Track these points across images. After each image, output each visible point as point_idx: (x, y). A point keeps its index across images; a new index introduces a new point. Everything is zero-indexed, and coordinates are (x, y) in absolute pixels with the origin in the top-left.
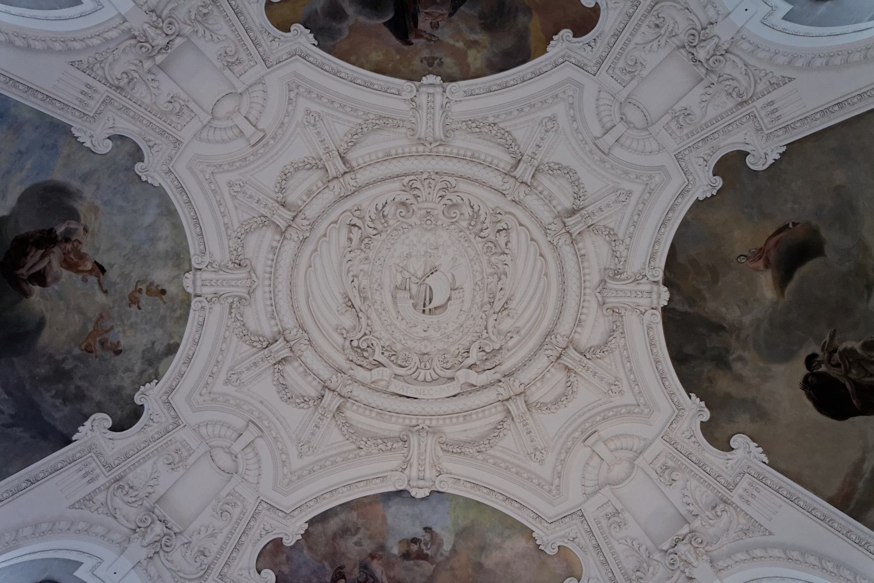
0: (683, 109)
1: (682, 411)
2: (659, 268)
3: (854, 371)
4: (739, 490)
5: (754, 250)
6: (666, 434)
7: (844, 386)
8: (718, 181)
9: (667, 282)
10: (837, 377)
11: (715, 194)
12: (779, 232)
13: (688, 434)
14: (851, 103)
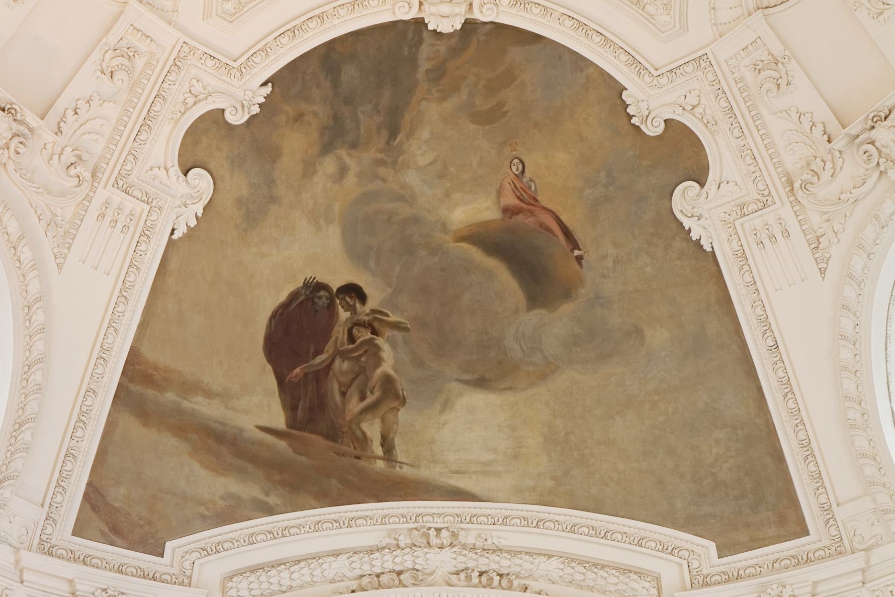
0: (790, 79)
1: (238, 75)
2: (497, 13)
3: (346, 365)
4: (118, 197)
5: (533, 189)
6: (193, 50)
7: (318, 352)
8: (656, 130)
9: (470, 26)
10: (333, 338)
11: (633, 121)
12: (567, 233)
13: (198, 88)
14: (776, 367)
